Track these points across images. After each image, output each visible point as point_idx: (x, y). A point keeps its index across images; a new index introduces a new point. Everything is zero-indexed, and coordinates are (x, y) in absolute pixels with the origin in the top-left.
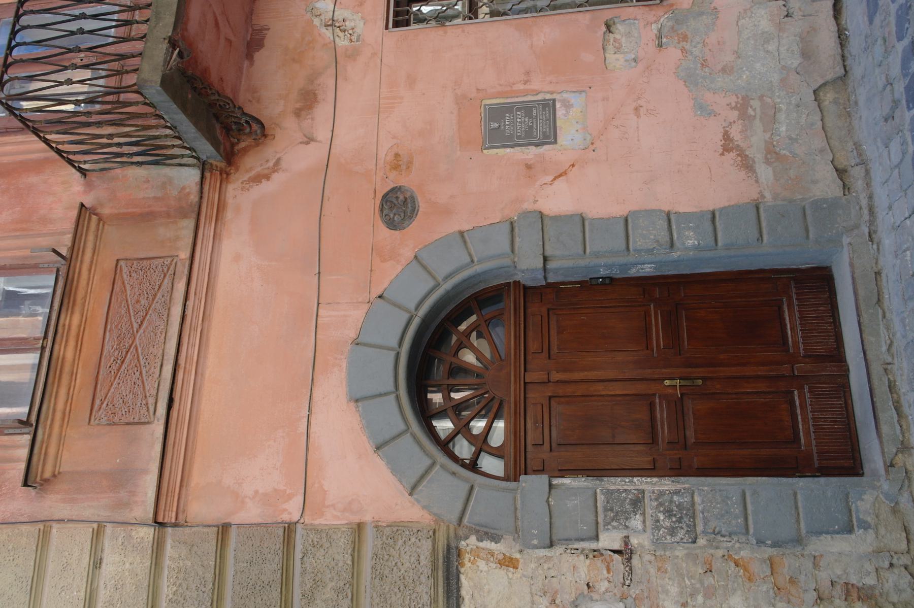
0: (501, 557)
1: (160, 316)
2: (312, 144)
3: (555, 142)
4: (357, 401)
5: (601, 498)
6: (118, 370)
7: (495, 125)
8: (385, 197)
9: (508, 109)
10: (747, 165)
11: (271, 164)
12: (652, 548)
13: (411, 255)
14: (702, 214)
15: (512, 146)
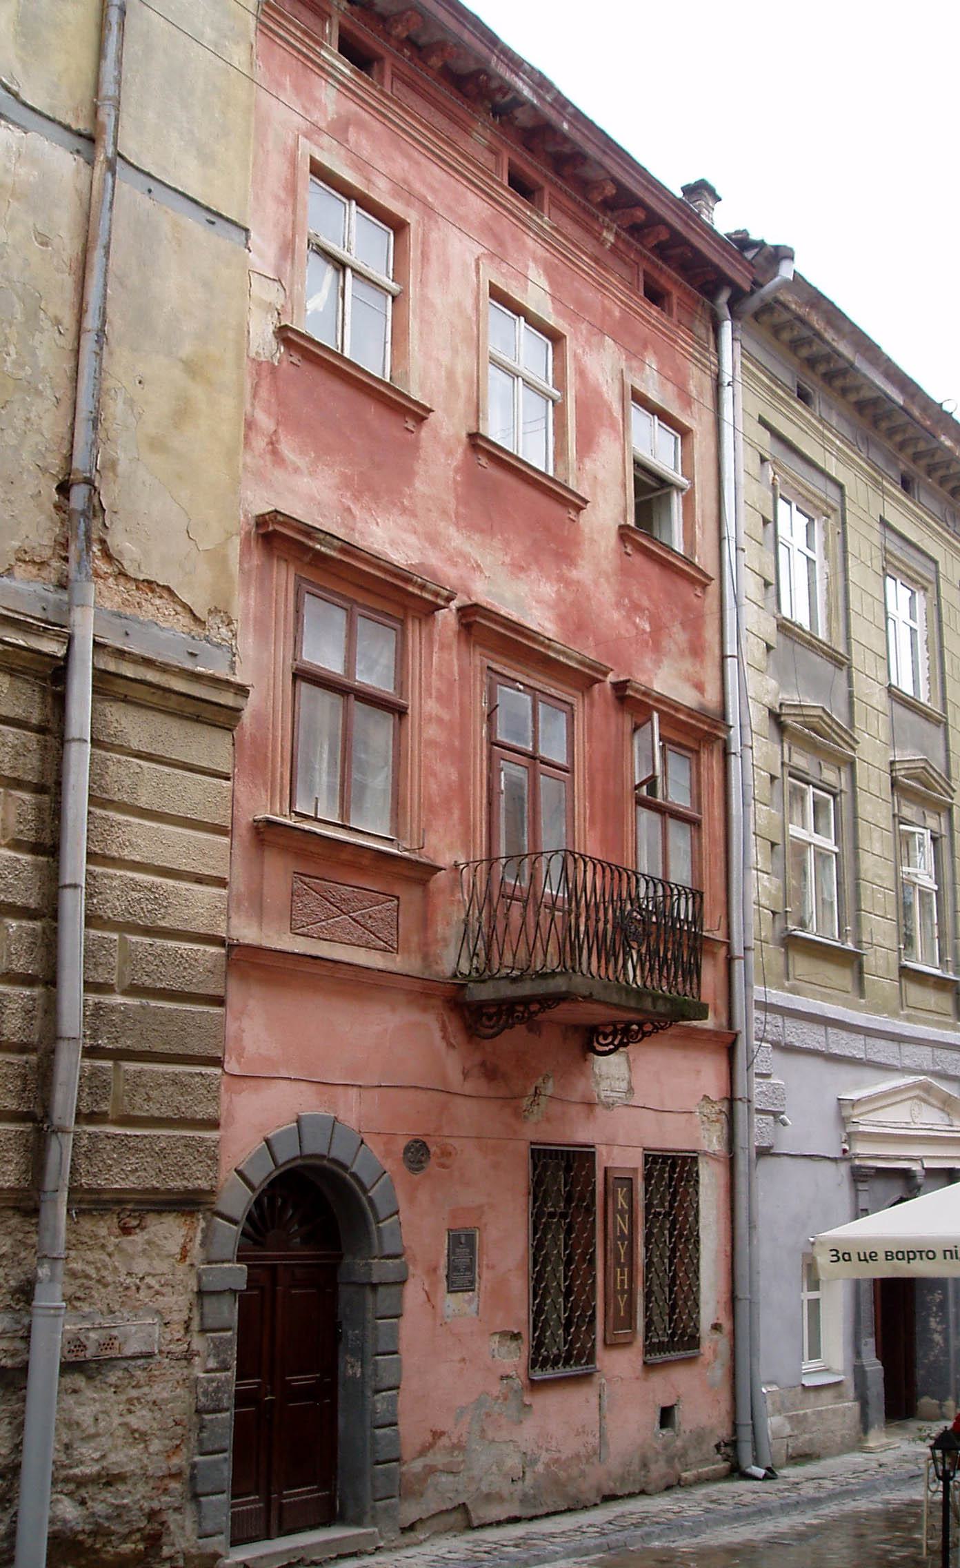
0: (188, 1248)
1: (360, 938)
2: (461, 1077)
3: (449, 1292)
4: (297, 1122)
6: (326, 899)
8: (424, 1143)
9: (472, 1253)
10: (423, 1452)
11: (452, 1041)
12: (192, 1377)
13: (387, 1167)
14: (395, 1414)
15: (448, 1255)
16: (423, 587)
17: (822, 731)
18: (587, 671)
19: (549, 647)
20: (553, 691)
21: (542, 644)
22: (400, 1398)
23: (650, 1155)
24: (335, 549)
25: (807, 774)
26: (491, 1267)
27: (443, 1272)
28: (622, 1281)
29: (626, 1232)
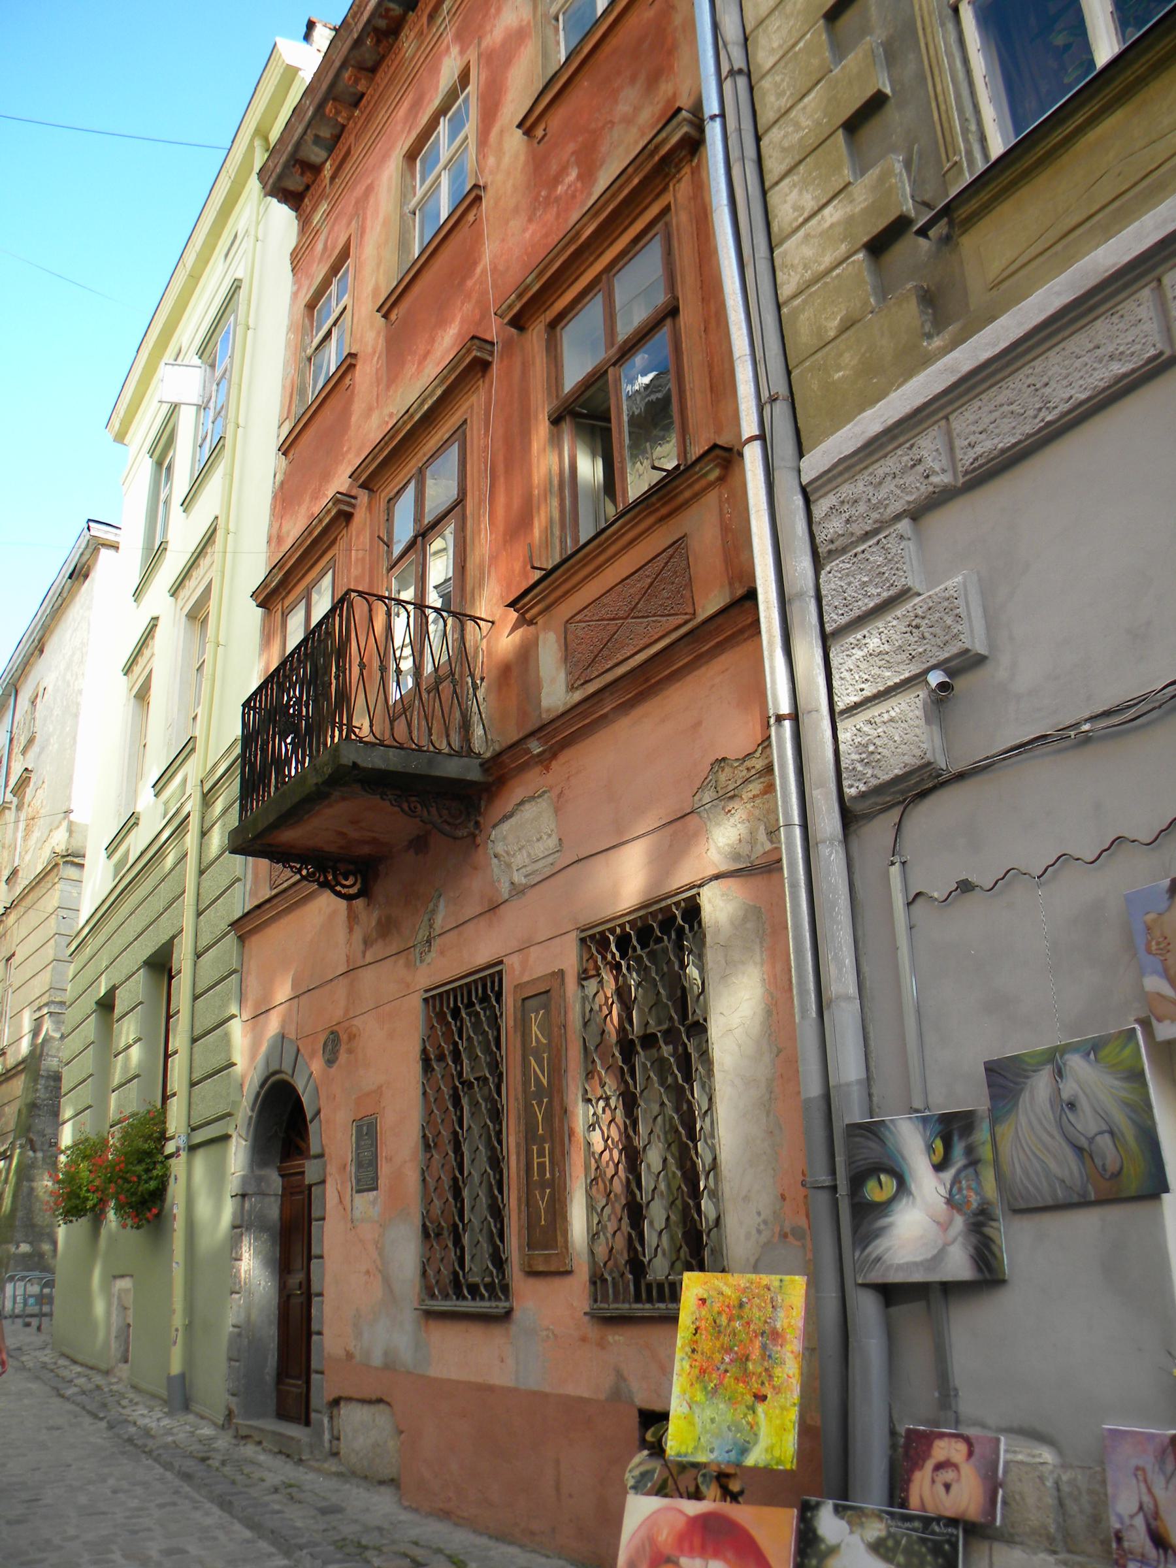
3: (358, 1191)
19: (412, 416)
23: (592, 937)
24: (278, 573)
28: (541, 1166)
29: (545, 1082)
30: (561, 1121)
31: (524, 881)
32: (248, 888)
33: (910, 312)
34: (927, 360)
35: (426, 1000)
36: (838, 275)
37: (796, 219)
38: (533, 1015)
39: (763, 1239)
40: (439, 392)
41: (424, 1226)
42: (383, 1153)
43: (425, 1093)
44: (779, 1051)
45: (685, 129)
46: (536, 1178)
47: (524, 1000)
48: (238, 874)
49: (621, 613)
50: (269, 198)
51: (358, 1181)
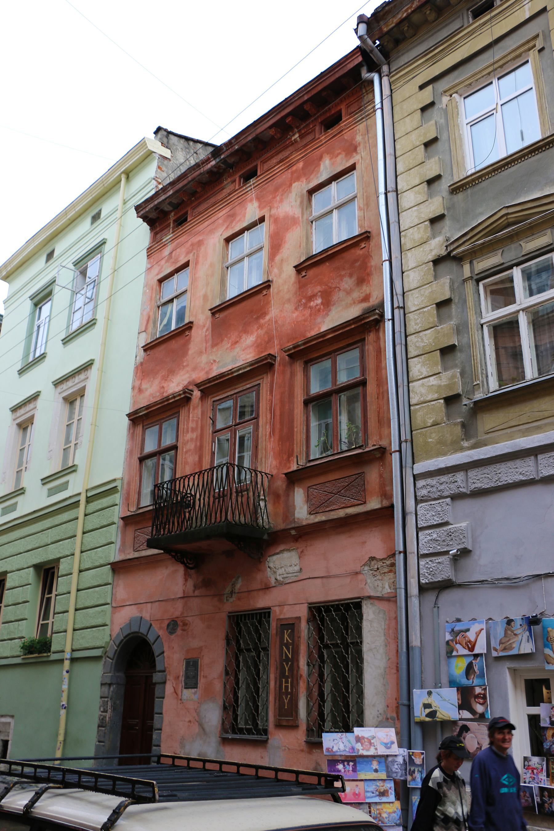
3: (185, 688)
5: (106, 699)
7: (191, 663)
16: (174, 397)
17: (519, 218)
18: (256, 365)
19: (232, 373)
20: (248, 386)
21: (228, 374)
22: (162, 735)
23: (314, 607)
24: (144, 410)
25: (503, 264)
26: (205, 677)
27: (182, 679)
28: (287, 687)
29: (290, 656)
30: (297, 671)
31: (282, 580)
32: (118, 547)
33: (458, 430)
34: (462, 449)
35: (229, 617)
36: (433, 405)
37: (419, 376)
38: (285, 631)
39: (379, 719)
40: (248, 369)
41: (224, 705)
42: (201, 674)
43: (227, 652)
44: (389, 659)
45: (377, 317)
46: (284, 690)
47: (281, 625)
48: (113, 540)
49: (334, 492)
50: (139, 218)
51: (186, 684)
